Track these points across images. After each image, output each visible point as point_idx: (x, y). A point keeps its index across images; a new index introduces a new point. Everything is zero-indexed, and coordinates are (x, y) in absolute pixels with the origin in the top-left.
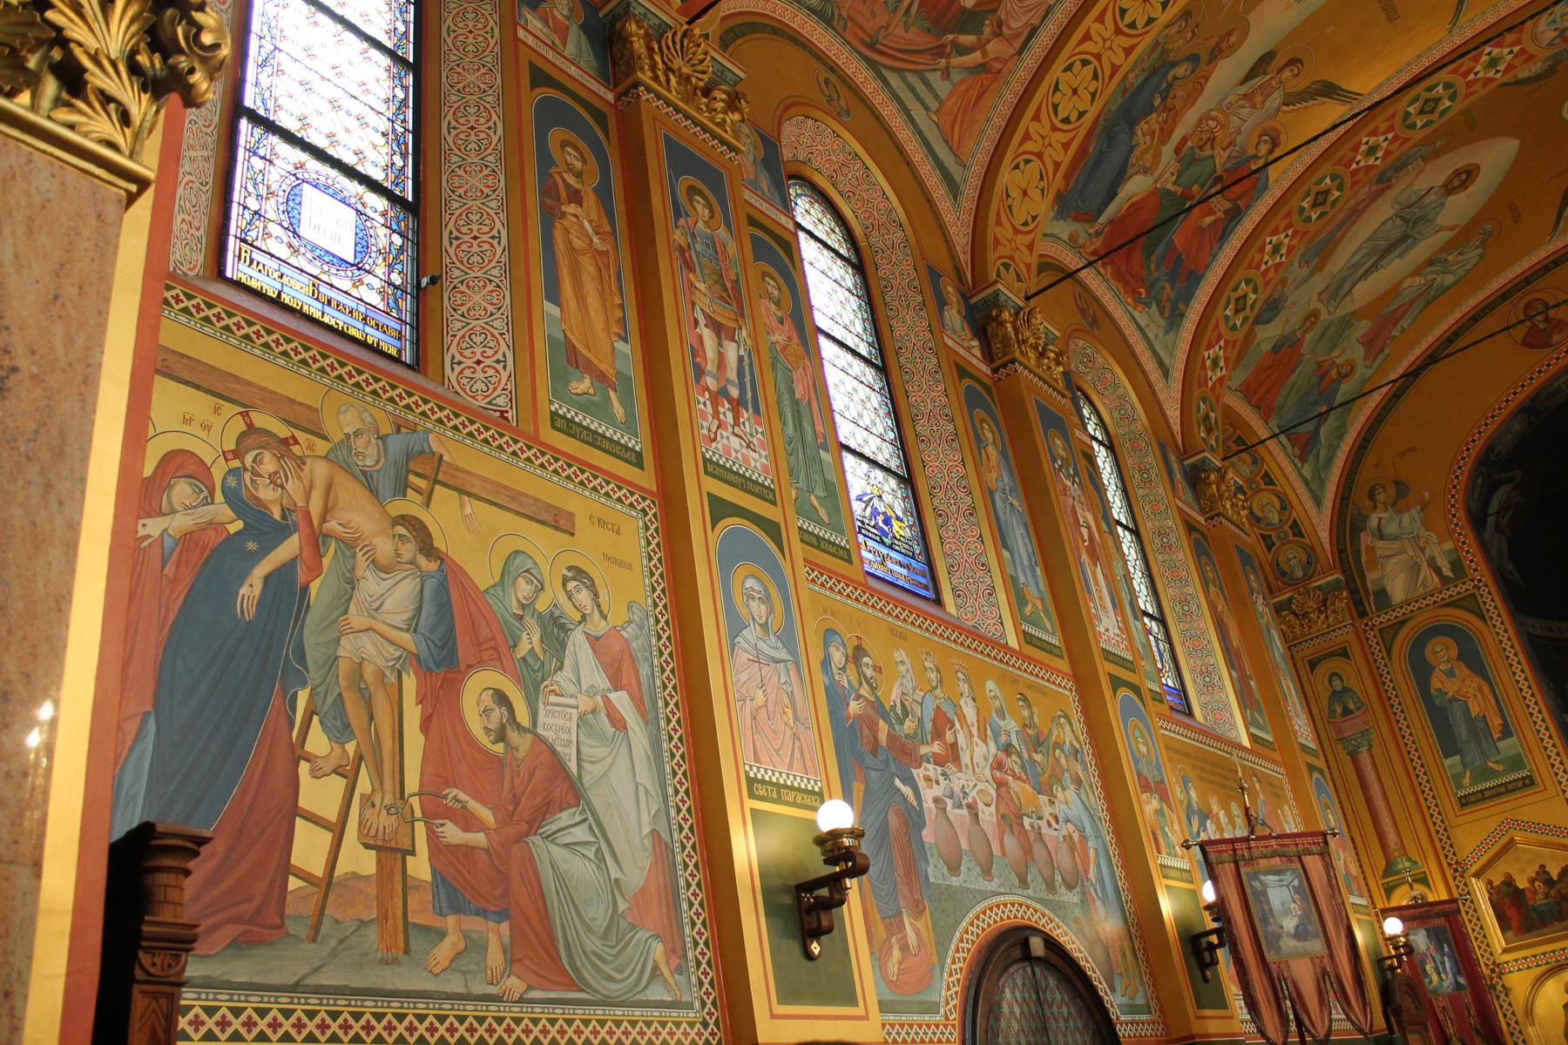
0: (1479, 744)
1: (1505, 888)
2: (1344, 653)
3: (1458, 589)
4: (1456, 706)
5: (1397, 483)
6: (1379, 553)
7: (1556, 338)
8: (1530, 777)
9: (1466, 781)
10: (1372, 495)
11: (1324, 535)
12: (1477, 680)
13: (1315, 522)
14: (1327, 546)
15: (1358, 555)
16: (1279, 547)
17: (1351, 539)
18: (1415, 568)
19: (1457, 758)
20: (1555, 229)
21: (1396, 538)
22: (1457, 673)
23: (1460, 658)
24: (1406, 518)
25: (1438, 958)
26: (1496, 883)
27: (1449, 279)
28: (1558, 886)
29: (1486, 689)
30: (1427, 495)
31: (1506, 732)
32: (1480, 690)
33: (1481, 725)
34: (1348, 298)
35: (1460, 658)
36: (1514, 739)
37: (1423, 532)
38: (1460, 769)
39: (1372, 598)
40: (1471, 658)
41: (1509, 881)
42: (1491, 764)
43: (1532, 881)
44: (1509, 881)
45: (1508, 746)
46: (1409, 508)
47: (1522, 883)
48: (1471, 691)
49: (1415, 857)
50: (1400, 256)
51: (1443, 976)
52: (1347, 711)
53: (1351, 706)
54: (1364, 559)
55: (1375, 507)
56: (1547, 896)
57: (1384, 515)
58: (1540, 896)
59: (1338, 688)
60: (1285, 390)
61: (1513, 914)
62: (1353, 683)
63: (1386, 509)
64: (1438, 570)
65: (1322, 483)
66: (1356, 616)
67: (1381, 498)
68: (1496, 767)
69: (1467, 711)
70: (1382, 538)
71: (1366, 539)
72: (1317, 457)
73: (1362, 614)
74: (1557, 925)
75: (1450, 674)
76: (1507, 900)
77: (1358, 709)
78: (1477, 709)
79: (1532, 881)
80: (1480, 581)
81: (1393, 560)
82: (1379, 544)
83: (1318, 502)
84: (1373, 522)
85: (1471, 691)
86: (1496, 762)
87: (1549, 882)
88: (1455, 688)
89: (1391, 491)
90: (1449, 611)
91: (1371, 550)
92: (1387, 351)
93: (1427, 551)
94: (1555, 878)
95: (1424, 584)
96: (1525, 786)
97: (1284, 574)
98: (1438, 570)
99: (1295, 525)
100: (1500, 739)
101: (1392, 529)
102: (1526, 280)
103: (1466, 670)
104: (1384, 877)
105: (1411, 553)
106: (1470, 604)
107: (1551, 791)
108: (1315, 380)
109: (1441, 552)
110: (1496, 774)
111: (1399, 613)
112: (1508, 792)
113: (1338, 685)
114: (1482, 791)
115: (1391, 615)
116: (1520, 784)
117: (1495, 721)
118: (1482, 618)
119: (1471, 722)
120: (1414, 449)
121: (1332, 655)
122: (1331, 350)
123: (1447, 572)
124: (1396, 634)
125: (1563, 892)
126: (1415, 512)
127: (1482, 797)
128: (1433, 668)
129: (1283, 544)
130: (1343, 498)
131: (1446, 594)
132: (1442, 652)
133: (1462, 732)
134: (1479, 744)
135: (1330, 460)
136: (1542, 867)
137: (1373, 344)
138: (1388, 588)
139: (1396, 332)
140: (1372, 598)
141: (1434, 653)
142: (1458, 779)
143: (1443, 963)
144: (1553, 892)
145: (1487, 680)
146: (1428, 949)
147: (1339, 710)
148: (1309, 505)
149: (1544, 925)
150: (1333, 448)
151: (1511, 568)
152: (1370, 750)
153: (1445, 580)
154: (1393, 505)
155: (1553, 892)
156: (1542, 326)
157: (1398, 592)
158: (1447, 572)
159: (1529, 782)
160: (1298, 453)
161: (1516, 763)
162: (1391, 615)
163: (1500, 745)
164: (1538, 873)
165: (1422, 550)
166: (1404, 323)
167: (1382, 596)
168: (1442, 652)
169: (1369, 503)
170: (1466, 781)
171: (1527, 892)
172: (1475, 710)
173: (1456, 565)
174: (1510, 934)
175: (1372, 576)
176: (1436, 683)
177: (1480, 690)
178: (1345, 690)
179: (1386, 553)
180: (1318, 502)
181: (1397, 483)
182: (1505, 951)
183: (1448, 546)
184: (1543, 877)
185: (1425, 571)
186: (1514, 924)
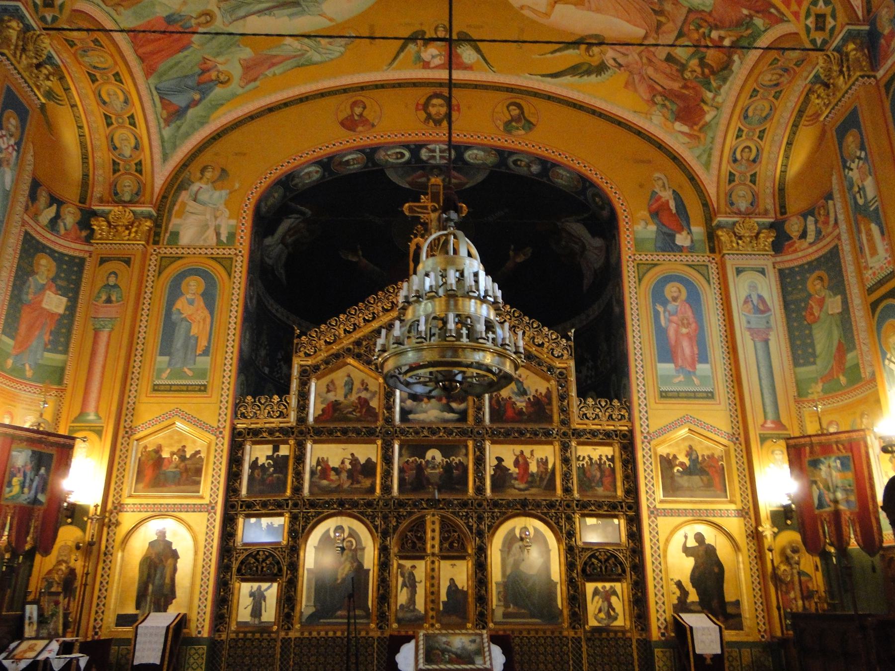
0: (186, 354)
1: (153, 455)
2: (128, 262)
3: (224, 252)
4: (184, 324)
5: (223, 170)
6: (188, 208)
7: (360, 128)
8: (205, 386)
9: (165, 375)
10: (203, 170)
11: (159, 181)
12: (206, 313)
13: (156, 169)
14: (157, 190)
15: (174, 204)
16: (122, 174)
17: (176, 191)
18: (205, 227)
19: (166, 358)
20: (391, 64)
21: (203, 204)
22: (196, 304)
23: (203, 295)
24: (217, 194)
25: (30, 475)
26: (149, 449)
27: (317, 58)
28: (187, 462)
29: (208, 320)
30: (237, 186)
31: (206, 352)
32: (204, 320)
33: (193, 341)
34: (241, 22)
35: (203, 295)
36: (208, 359)
37: (222, 207)
38: (164, 366)
39: (168, 235)
40: (209, 298)
41: (158, 450)
42: (186, 370)
43: (173, 454)
44: (158, 450)
45: (203, 362)
46: (222, 188)
47: (165, 455)
48: (198, 318)
49: (102, 415)
50: (291, 15)
51: (26, 490)
52: (109, 301)
53: (114, 298)
54: (176, 208)
55: (201, 179)
56: (176, 467)
57: (204, 186)
58: (173, 465)
59: (111, 283)
60: (171, 61)
61: (149, 473)
62: (123, 284)
63: (207, 184)
64: (218, 234)
65: (175, 147)
66: (151, 241)
67: (208, 174)
68: (189, 373)
69: (189, 330)
70: (195, 201)
71: (184, 196)
72: (179, 127)
73: (156, 243)
74: (174, 488)
75: (191, 302)
76: (151, 462)
77: (118, 301)
78: (196, 331)
79: (173, 454)
80: (240, 252)
81: (194, 217)
82: (192, 203)
83: (165, 158)
84: (195, 187)
85: (198, 318)
86: (189, 369)
87: (183, 458)
88: (189, 313)
89: (217, 173)
90: (213, 263)
91: (184, 204)
92: (258, 83)
93: (219, 220)
94: (188, 456)
95: (205, 240)
96: (200, 390)
97: (116, 194)
98: (218, 234)
99: (139, 164)
100: (200, 355)
101: (203, 197)
102: (362, 88)
103: (202, 304)
104: (73, 422)
105: (208, 217)
106: (226, 263)
107: (214, 399)
108: (197, 70)
109: (226, 224)
110: (186, 377)
111: (179, 251)
112: (187, 391)
113: (112, 281)
114: (171, 385)
115: (174, 251)
116: (197, 388)
117: (203, 343)
118: (229, 275)
119: (188, 338)
120: (245, 154)
121: (119, 259)
122: (218, 54)
123: (224, 238)
124: (172, 263)
125: (188, 466)
126: (224, 193)
127: (170, 389)
128: (182, 294)
129: (126, 174)
130: (185, 165)
131: (215, 251)
132: (193, 286)
133: (178, 343)
134: (186, 354)
135: (187, 135)
136: (184, 447)
137: (251, 70)
138: (181, 234)
139: (269, 73)
140: (168, 235)
141: (188, 285)
142: (160, 371)
143: (32, 481)
144: (182, 465)
145: (212, 313)
146: (25, 466)
147: (104, 297)
148: (158, 156)
149: (164, 486)
150: (193, 129)
151: (282, 271)
152: (110, 333)
153: (219, 242)
154: (213, 182)
155: (182, 465)
156: (356, 118)
157: (185, 238)
158: (224, 238)
159: (203, 389)
160: (165, 116)
161: (202, 374)
162: (174, 251)
163: (198, 359)
164: (179, 450)
165: (216, 218)
166: (277, 70)
167: (175, 235)
168: (193, 286)
169: (199, 175)
170: (165, 375)
171: (166, 462)
172: (194, 331)
173: (232, 236)
174: (141, 486)
175: (175, 221)
176: (181, 304)
177: (204, 320)
178: (116, 286)
179: (191, 210)
180: (165, 158)
181: (223, 170)
182: (130, 496)
183: (233, 222)
184: (181, 453)
185: (211, 233)
186: (147, 479)
